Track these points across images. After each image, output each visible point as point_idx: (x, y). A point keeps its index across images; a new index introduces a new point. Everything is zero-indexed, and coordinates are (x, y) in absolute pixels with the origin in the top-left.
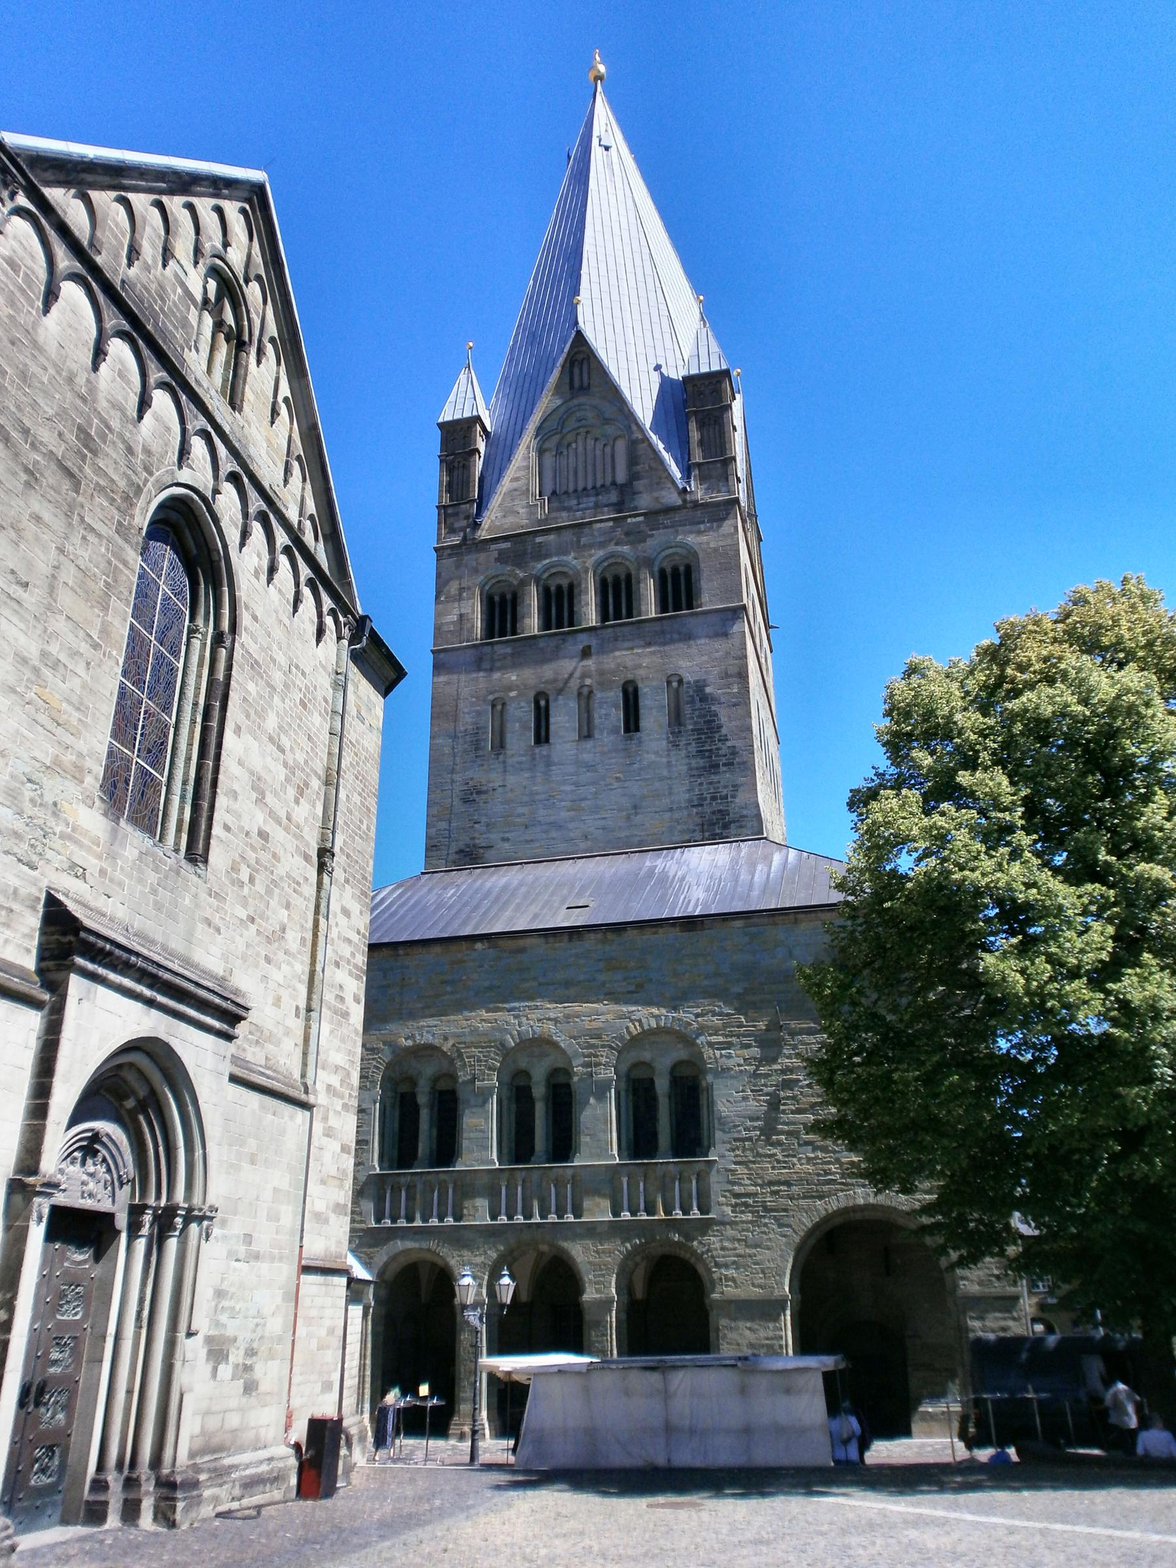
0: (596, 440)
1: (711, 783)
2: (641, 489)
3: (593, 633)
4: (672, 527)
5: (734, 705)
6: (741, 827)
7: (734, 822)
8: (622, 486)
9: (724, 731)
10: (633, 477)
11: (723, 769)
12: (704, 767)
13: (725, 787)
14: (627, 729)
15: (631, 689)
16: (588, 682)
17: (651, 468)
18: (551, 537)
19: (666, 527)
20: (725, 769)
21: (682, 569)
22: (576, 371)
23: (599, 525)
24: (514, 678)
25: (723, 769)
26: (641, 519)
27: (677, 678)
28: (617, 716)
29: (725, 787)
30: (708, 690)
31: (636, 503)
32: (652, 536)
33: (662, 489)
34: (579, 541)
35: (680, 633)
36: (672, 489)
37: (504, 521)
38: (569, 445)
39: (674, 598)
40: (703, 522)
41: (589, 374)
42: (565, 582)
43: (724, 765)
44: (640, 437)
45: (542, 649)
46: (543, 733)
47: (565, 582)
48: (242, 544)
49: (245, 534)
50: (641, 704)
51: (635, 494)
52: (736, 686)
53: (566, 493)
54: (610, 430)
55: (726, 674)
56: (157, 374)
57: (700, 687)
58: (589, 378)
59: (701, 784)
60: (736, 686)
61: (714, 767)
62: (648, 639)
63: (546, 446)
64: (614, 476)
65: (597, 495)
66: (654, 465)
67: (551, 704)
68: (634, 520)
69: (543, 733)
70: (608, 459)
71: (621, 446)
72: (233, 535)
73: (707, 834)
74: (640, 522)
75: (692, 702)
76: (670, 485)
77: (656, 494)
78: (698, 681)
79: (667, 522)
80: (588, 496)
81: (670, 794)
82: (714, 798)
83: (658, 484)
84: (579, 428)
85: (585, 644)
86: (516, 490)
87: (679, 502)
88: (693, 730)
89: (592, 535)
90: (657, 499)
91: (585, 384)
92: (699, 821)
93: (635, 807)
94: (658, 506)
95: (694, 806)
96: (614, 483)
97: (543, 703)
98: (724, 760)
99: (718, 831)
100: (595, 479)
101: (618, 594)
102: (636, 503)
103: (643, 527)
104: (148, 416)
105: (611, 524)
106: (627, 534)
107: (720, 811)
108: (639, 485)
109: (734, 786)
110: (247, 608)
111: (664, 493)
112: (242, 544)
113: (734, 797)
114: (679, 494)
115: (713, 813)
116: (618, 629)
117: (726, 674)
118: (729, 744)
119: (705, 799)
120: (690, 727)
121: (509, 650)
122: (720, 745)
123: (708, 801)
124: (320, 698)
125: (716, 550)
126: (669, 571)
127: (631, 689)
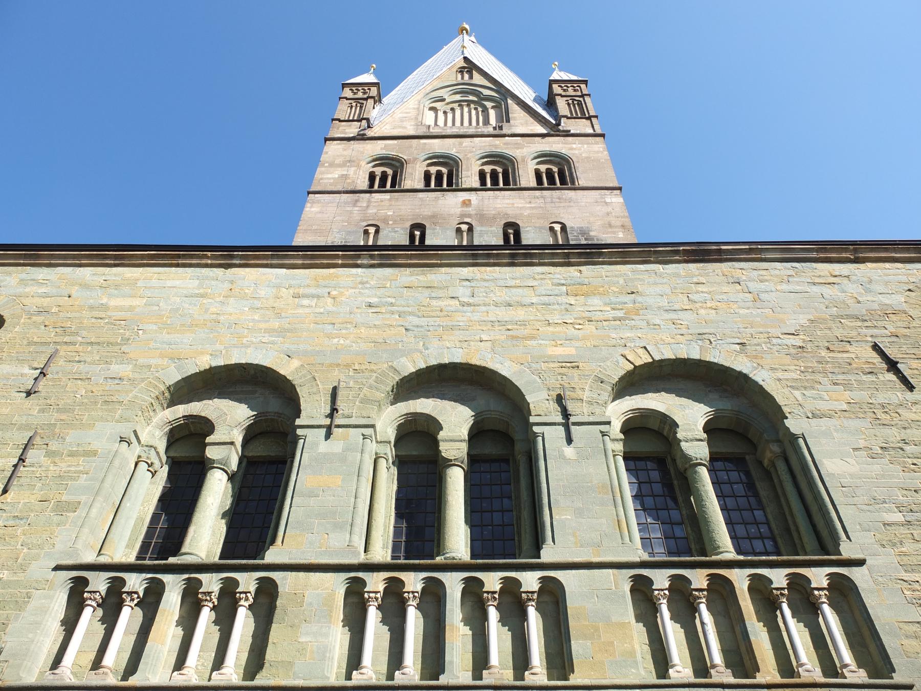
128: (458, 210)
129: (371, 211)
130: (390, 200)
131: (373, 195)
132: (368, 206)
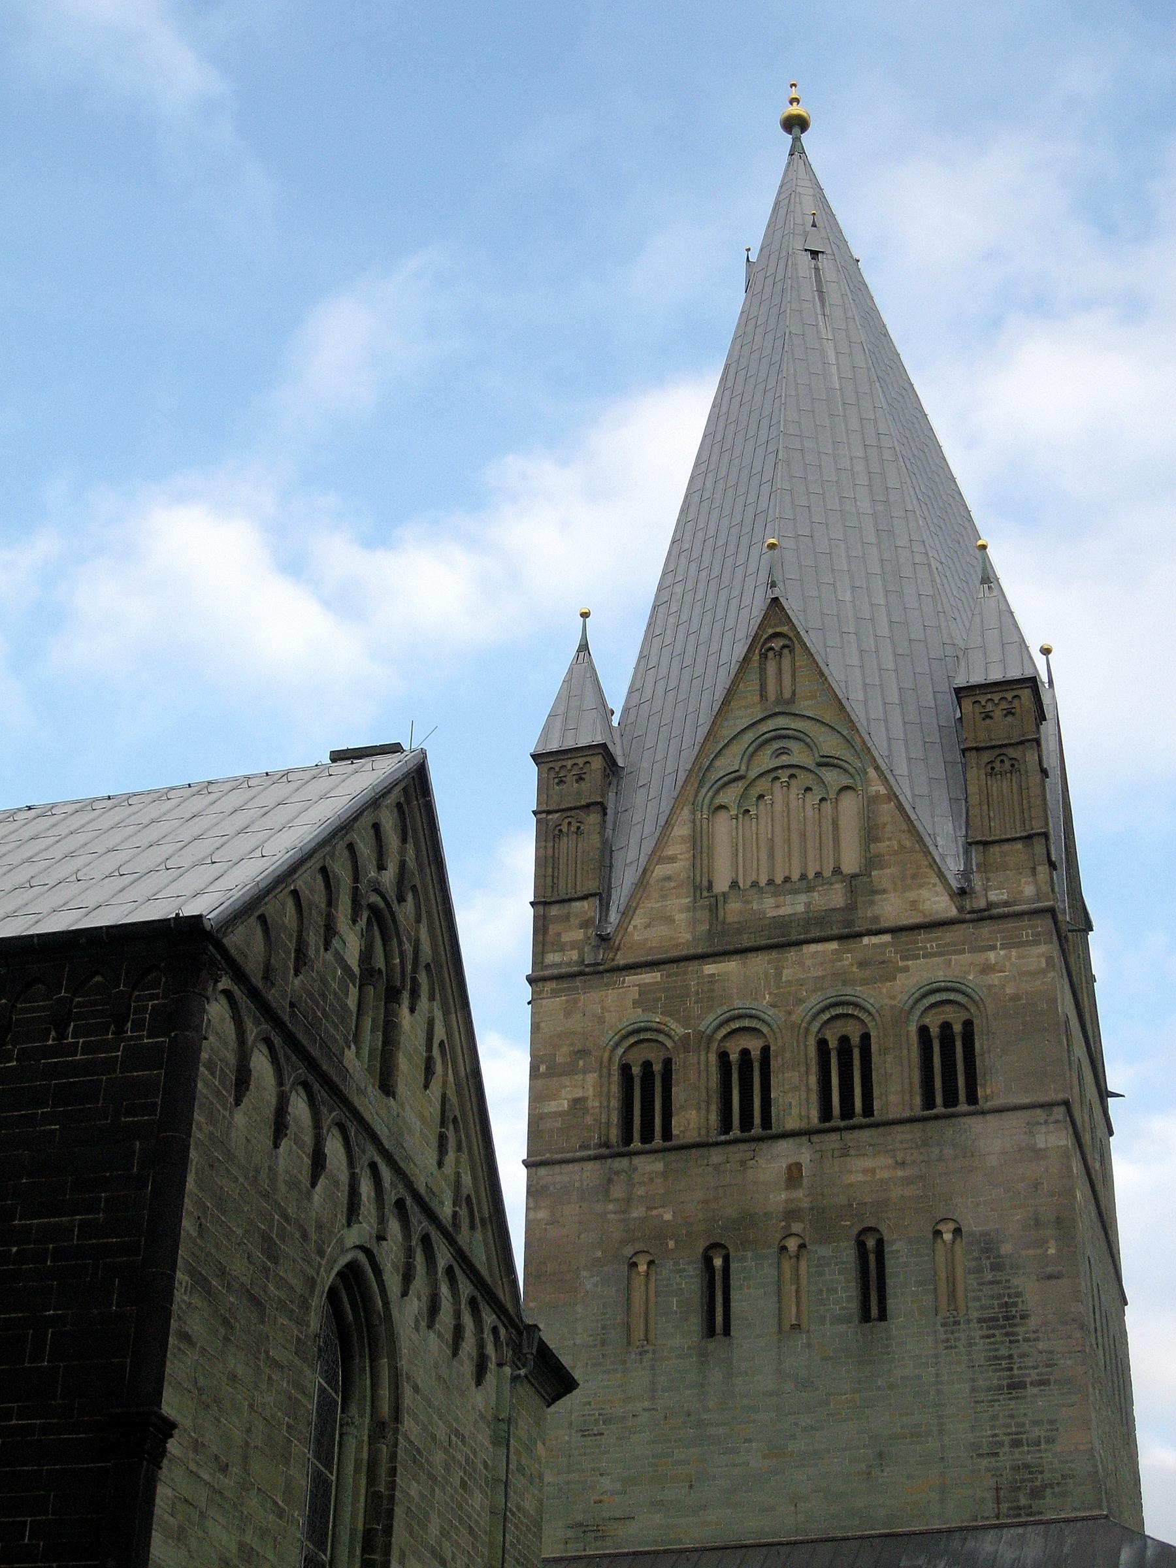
0: (808, 789)
1: (1012, 1416)
2: (886, 883)
3: (805, 1139)
4: (940, 954)
5: (1050, 1277)
6: (1064, 1494)
7: (1051, 1485)
8: (854, 876)
9: (1033, 1322)
10: (871, 862)
11: (1032, 1390)
12: (1000, 1388)
13: (1037, 1423)
14: (866, 1317)
15: (871, 1243)
16: (797, 1227)
17: (902, 847)
18: (731, 967)
19: (932, 955)
20: (1036, 1390)
21: (957, 1028)
22: (771, 666)
23: (813, 948)
24: (668, 1217)
25: (1032, 1390)
26: (887, 938)
27: (952, 1226)
28: (843, 1290)
29: (1037, 1423)
30: (1006, 1248)
31: (876, 910)
32: (906, 969)
33: (921, 886)
34: (779, 975)
35: (954, 1145)
36: (940, 888)
37: (648, 934)
38: (761, 797)
39: (944, 1064)
40: (993, 948)
41: (794, 676)
42: (754, 1046)
43: (1032, 1384)
44: (883, 790)
45: (716, 1167)
46: (719, 1318)
47: (754, 1046)
48: (405, 1293)
49: (408, 1277)
50: (888, 1270)
51: (875, 892)
52: (1052, 1243)
53: (755, 884)
54: (829, 775)
55: (1037, 1220)
56: (329, 1117)
57: (987, 1245)
58: (794, 683)
59: (994, 1418)
60: (1052, 1243)
61: (1016, 1386)
62: (900, 1156)
63: (722, 799)
64: (837, 860)
65: (810, 889)
66: (908, 844)
67: (734, 1266)
68: (875, 940)
69: (719, 1318)
70: (827, 826)
71: (849, 805)
72: (393, 1283)
73: (1005, 1506)
74: (883, 945)
75: (979, 1270)
76: (935, 879)
77: (912, 895)
78: (987, 1233)
79: (931, 946)
80: (796, 892)
81: (941, 1432)
82: (1016, 1444)
83: (914, 876)
84: (776, 769)
85: (791, 1161)
86: (668, 878)
87: (953, 912)
88: (980, 1320)
89: (801, 963)
90: (914, 904)
91: (787, 694)
92: (991, 1483)
93: (880, 1455)
94: (917, 919)
95: (980, 1456)
96: (837, 871)
97: (718, 1262)
98: (1033, 1375)
99: (1023, 1501)
100: (805, 866)
101: (845, 1066)
102: (876, 910)
103: (890, 954)
104: (322, 1182)
105: (834, 945)
106: (862, 965)
107: (1027, 1466)
108: (882, 877)
109: (1051, 1422)
110: (408, 1378)
111: (925, 893)
112: (405, 1293)
113: (1049, 1441)
114: (952, 895)
115: (1016, 1469)
116: (848, 1135)
117: (1037, 1220)
118: (1041, 1345)
119: (1001, 1444)
120: (975, 1315)
121: (659, 1166)
122: (1025, 1347)
123: (1006, 1449)
124: (480, 1466)
125: (1016, 998)
126: (934, 1031)
127: (871, 1243)
128: (780, 1198)
129: (635, 1214)
130: (664, 1174)
131: (637, 1161)
132: (628, 1201)
